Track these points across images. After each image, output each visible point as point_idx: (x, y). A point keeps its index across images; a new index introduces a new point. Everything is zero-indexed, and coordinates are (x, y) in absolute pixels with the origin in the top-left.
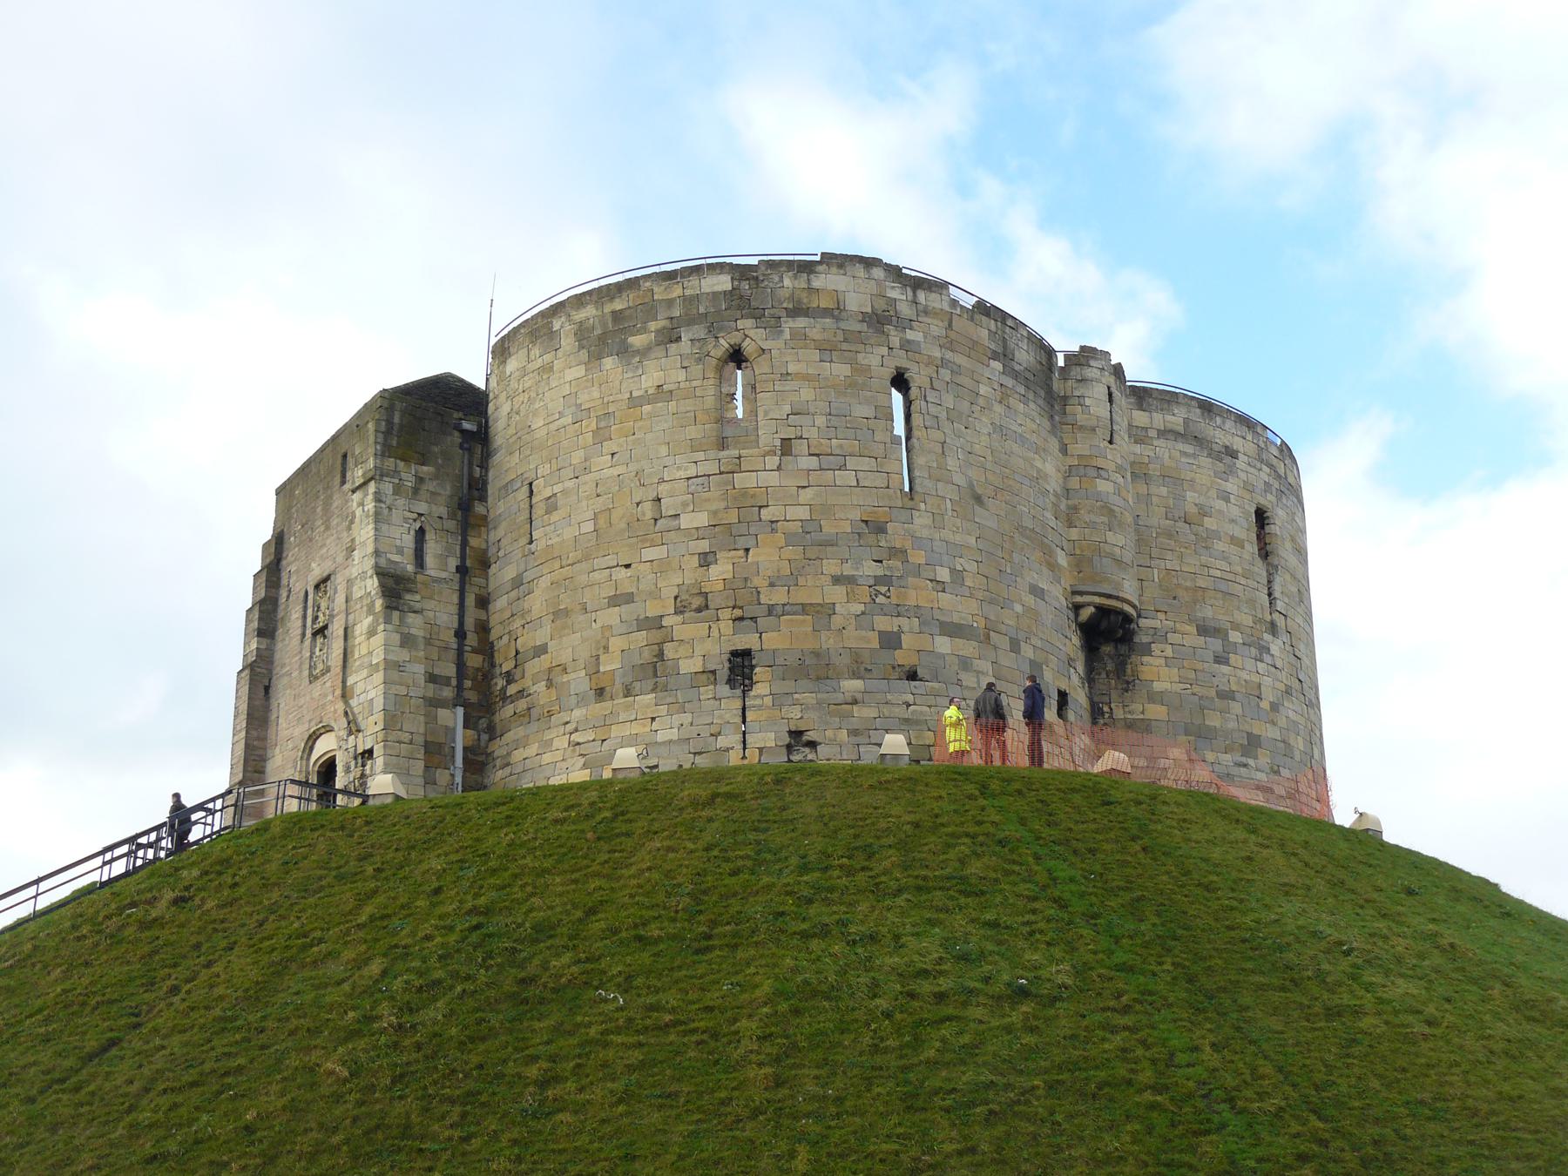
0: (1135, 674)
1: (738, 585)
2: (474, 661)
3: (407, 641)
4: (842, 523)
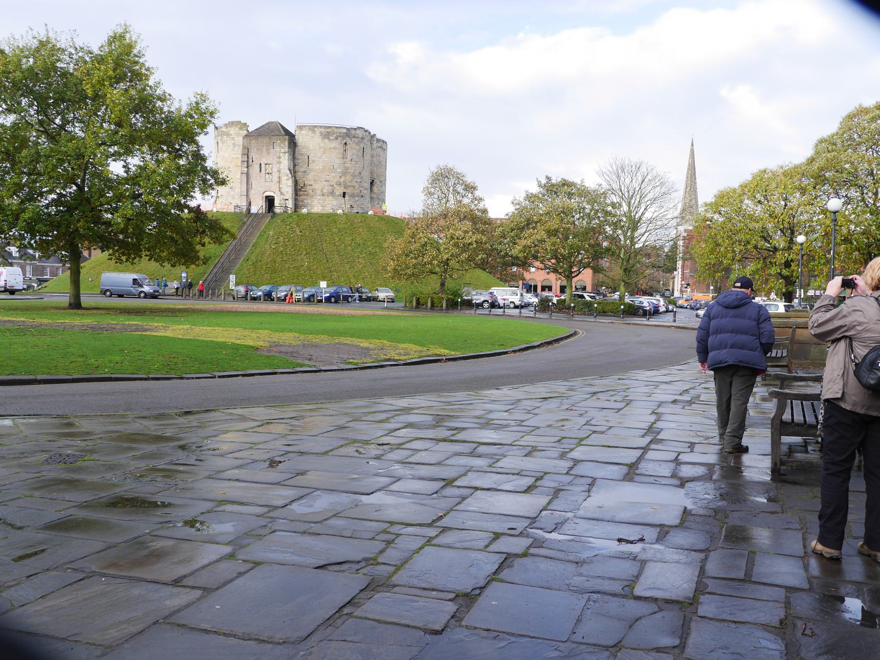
1: (344, 182)
4: (357, 173)
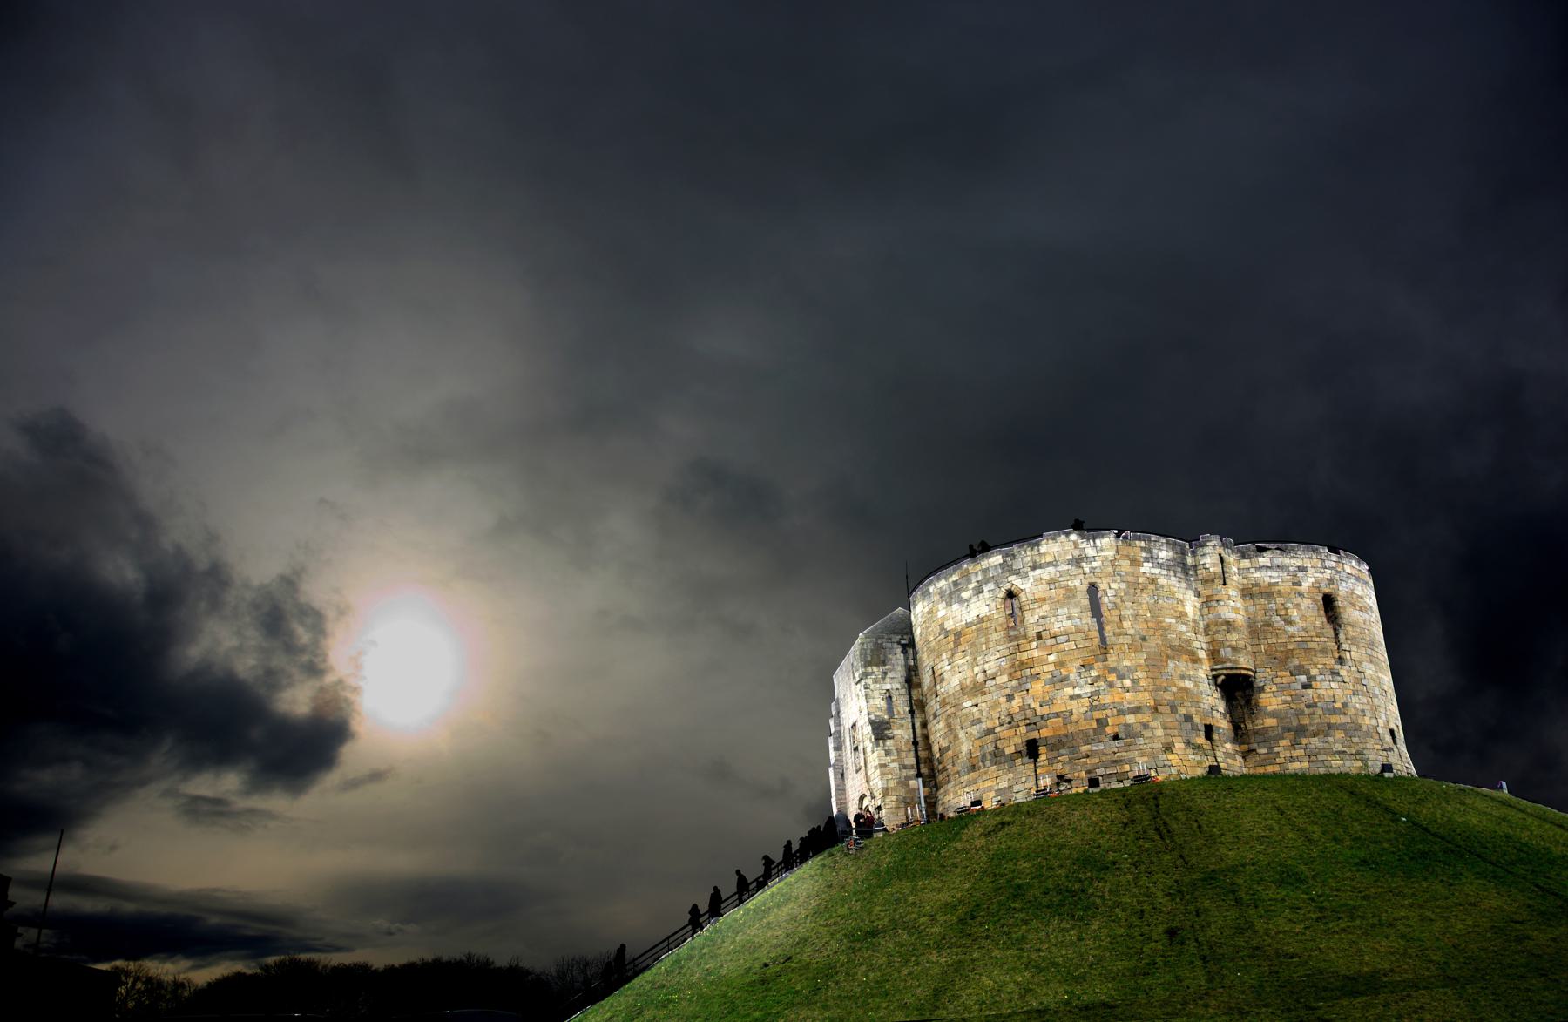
0: (1257, 705)
2: (922, 754)
3: (888, 753)
